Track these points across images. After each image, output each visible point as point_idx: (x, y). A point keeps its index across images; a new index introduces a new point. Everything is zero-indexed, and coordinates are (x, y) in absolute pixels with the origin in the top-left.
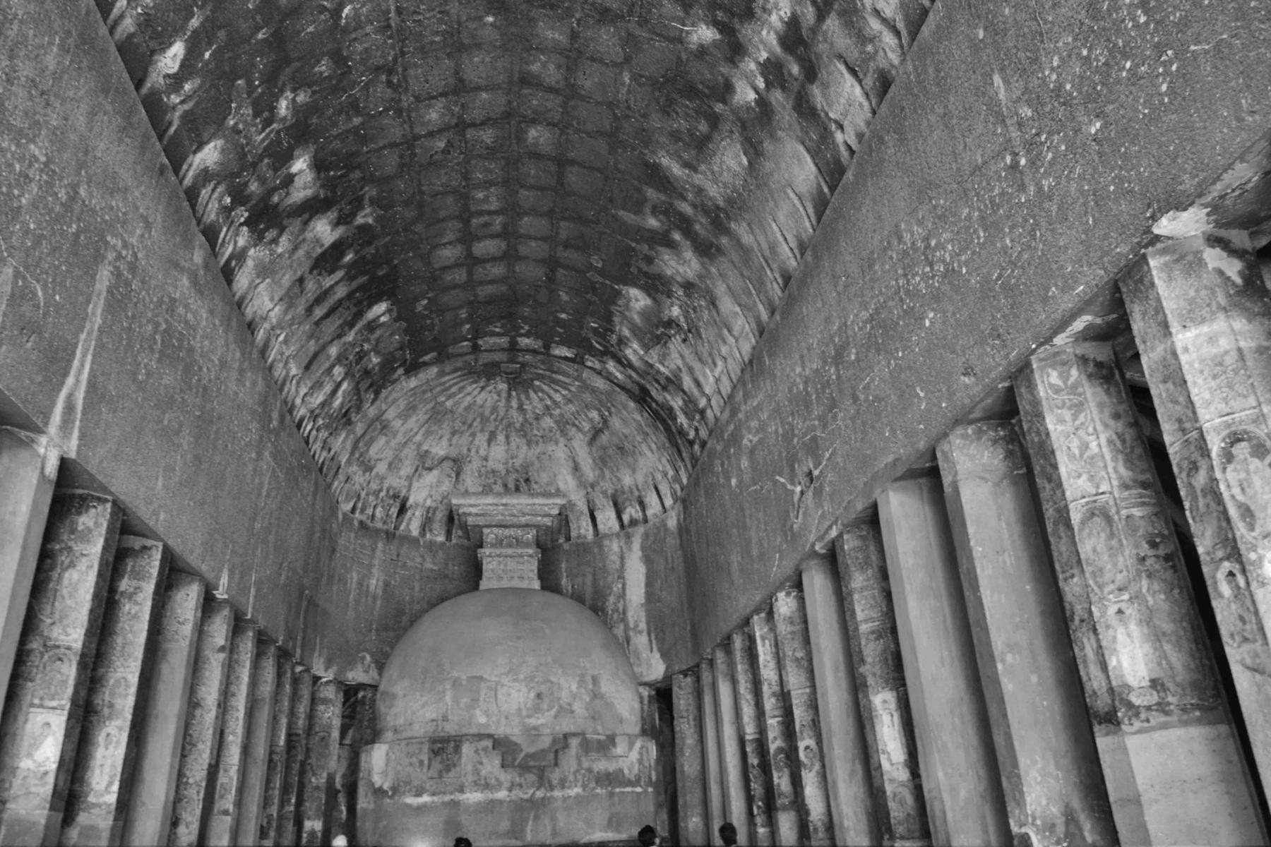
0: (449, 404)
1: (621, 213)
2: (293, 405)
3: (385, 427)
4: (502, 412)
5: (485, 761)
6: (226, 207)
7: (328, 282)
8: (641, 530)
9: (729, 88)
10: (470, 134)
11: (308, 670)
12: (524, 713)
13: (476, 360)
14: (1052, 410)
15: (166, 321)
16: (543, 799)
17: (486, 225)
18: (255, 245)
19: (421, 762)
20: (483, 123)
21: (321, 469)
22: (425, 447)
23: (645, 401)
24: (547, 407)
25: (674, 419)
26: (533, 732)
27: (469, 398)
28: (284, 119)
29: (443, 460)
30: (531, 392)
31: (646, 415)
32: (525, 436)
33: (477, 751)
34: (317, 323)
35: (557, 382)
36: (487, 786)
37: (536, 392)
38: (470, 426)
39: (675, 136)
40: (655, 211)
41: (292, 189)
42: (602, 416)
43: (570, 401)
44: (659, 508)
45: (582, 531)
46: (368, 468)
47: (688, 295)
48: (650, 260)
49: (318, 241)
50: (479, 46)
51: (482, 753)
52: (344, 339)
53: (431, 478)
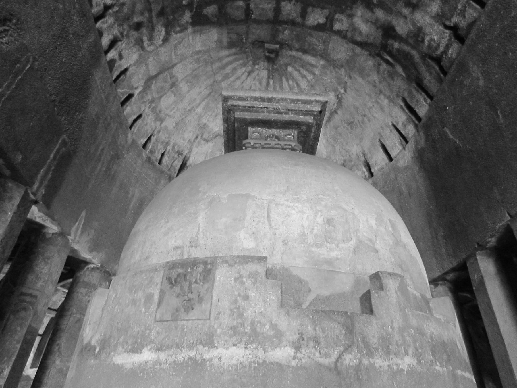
5: (252, 294)
11: (63, 234)
12: (310, 239)
13: (247, 33)
16: (358, 368)
19: (149, 298)
22: (205, 121)
23: (384, 47)
26: (325, 267)
30: (284, 79)
33: (239, 279)
36: (254, 337)
37: (287, 80)
42: (337, 97)
44: (387, 160)
51: (248, 283)
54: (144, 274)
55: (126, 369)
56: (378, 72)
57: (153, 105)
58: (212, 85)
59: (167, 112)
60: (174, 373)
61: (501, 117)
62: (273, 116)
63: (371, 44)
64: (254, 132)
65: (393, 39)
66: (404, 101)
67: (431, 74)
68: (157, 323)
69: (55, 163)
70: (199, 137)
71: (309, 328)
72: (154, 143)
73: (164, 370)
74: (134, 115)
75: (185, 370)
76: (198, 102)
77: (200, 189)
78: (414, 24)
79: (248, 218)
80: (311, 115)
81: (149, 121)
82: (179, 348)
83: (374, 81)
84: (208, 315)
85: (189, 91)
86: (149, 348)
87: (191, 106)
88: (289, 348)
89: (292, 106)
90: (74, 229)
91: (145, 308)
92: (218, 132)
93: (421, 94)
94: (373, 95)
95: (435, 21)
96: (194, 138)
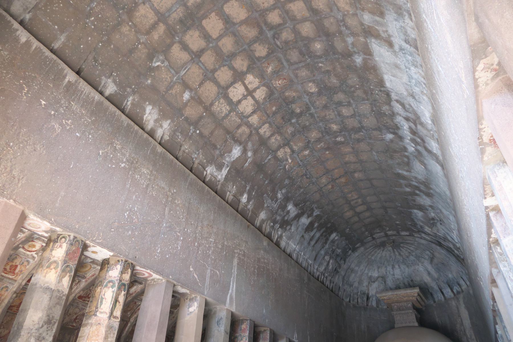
0: (373, 258)
1: (396, 189)
2: (314, 272)
3: (352, 271)
4: (394, 258)
6: (272, 226)
7: (312, 234)
8: (461, 296)
9: (405, 149)
10: (337, 181)
13: (376, 242)
14: (501, 262)
15: (258, 265)
17: (356, 203)
18: (284, 232)
20: (340, 177)
21: (332, 291)
22: (370, 274)
24: (410, 253)
25: (454, 251)
27: (380, 255)
28: (281, 198)
29: (378, 277)
32: (405, 264)
34: (313, 246)
35: (408, 243)
38: (384, 264)
39: (399, 164)
40: (406, 186)
41: (290, 214)
42: (431, 253)
43: (416, 249)
45: (439, 298)
46: (351, 286)
47: (433, 209)
48: (414, 201)
49: (304, 224)
50: (328, 159)
52: (325, 248)
53: (375, 285)
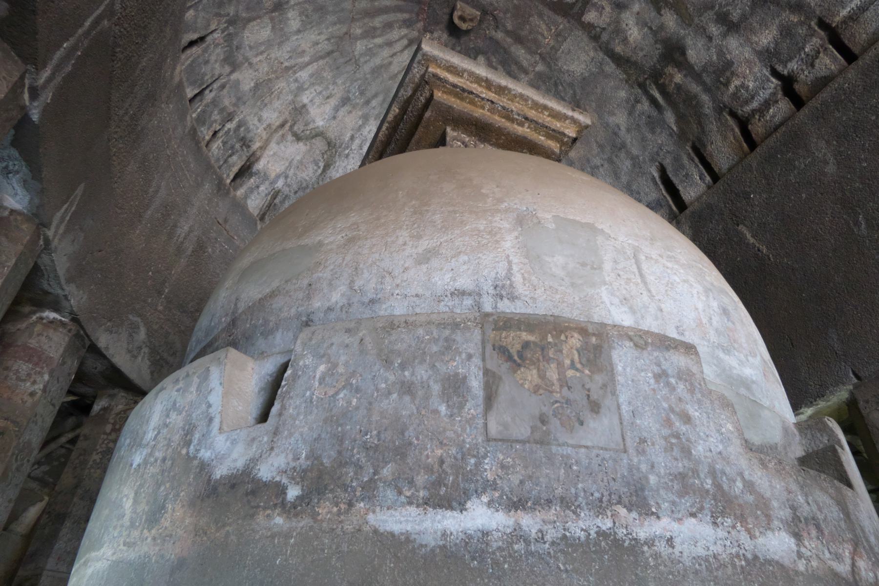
22: (305, 99)
23: (656, 76)
27: (386, 52)
31: (645, 106)
38: (367, 102)
53: (295, 150)
54: (421, 331)
55: (421, 546)
56: (630, 114)
57: (231, 29)
58: (341, 38)
59: (249, 54)
60: (569, 567)
61: (863, 226)
62: (498, 121)
63: (635, 64)
64: (455, 139)
65: (677, 67)
66: (663, 171)
67: (725, 138)
68: (492, 443)
69: (86, 43)
70: (287, 127)
71: (800, 497)
72: (207, 105)
73: (541, 558)
74: (195, 32)
75: (594, 560)
76: (307, 59)
77: (483, 191)
78: (721, 53)
79: (608, 266)
80: (557, 140)
81: (213, 58)
82: (569, 508)
83: (618, 126)
84: (620, 440)
85: (299, 31)
86: (485, 499)
87: (292, 62)
88: (784, 534)
89: (532, 114)
90: (59, 215)
91: (448, 406)
92: (321, 129)
93: (697, 166)
94: (608, 149)
95: (759, 58)
96: (278, 123)
